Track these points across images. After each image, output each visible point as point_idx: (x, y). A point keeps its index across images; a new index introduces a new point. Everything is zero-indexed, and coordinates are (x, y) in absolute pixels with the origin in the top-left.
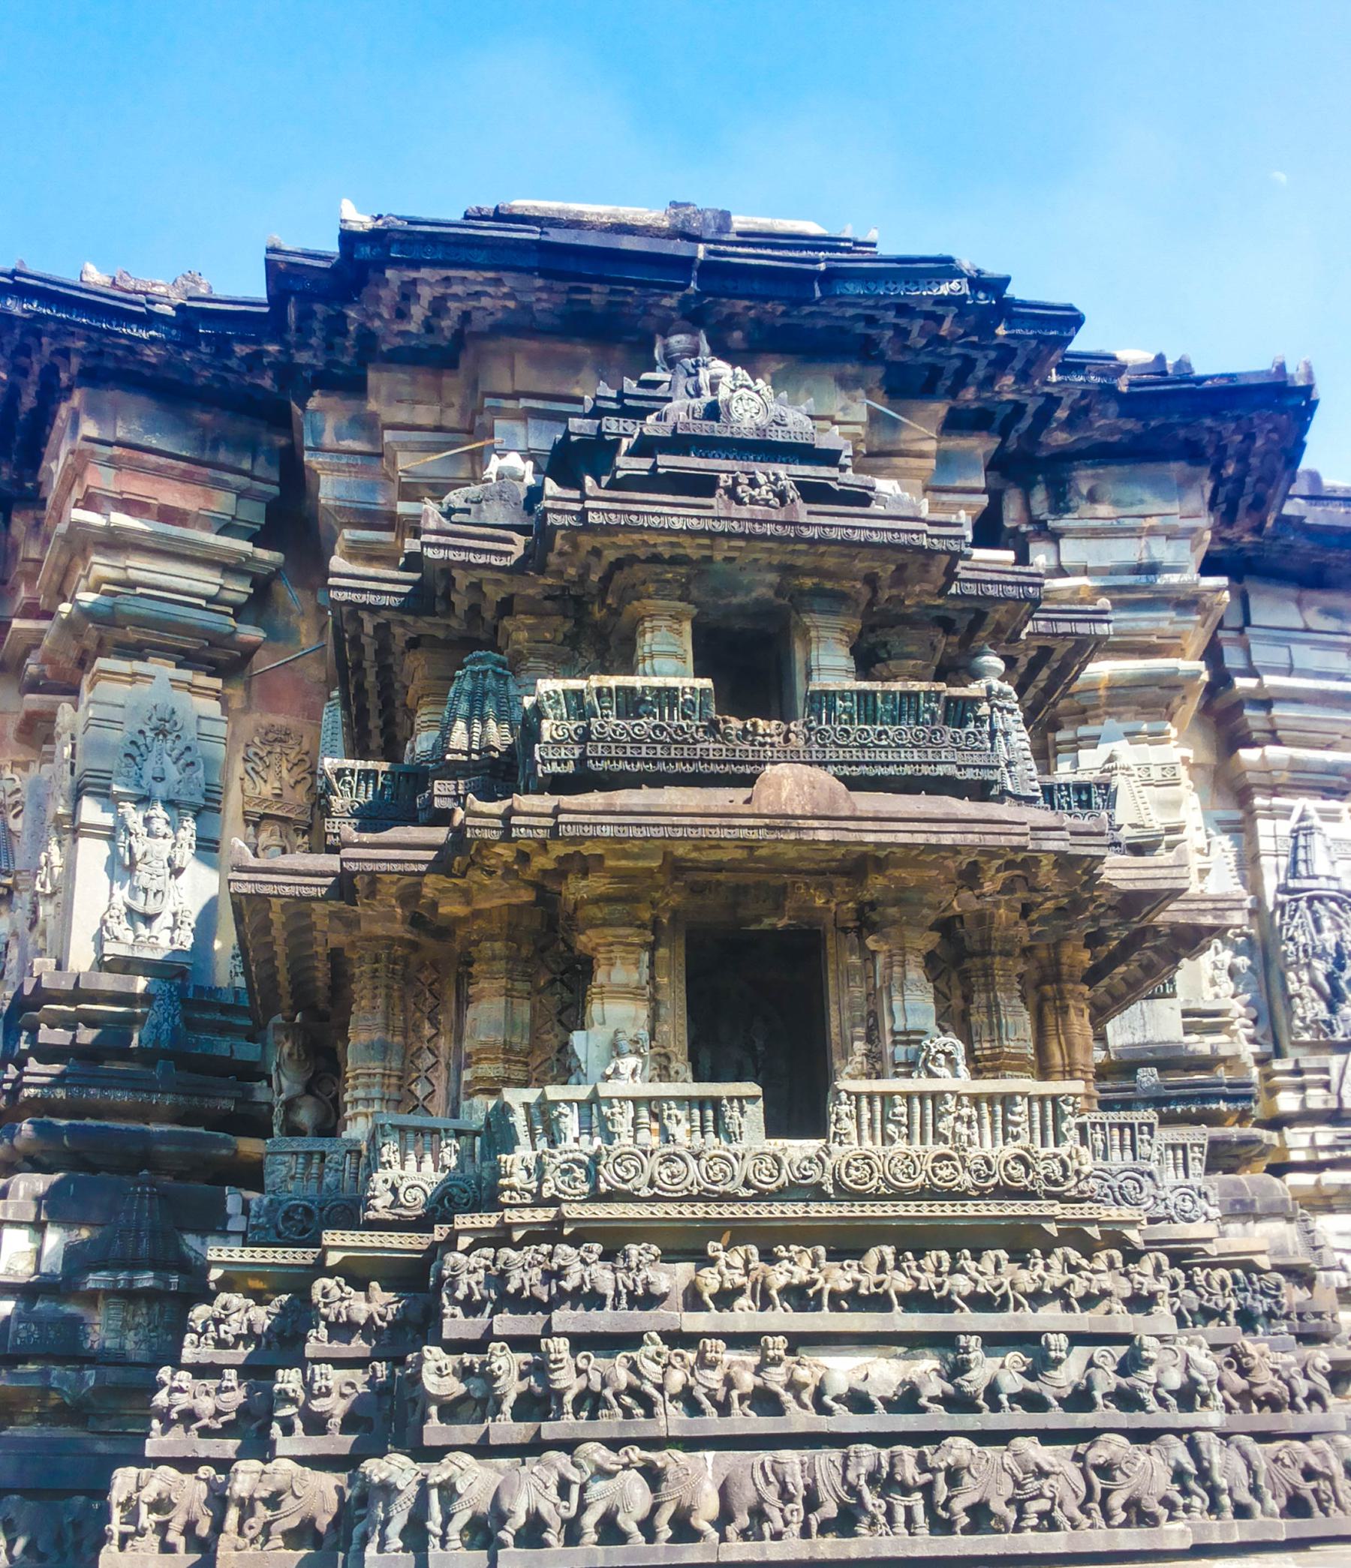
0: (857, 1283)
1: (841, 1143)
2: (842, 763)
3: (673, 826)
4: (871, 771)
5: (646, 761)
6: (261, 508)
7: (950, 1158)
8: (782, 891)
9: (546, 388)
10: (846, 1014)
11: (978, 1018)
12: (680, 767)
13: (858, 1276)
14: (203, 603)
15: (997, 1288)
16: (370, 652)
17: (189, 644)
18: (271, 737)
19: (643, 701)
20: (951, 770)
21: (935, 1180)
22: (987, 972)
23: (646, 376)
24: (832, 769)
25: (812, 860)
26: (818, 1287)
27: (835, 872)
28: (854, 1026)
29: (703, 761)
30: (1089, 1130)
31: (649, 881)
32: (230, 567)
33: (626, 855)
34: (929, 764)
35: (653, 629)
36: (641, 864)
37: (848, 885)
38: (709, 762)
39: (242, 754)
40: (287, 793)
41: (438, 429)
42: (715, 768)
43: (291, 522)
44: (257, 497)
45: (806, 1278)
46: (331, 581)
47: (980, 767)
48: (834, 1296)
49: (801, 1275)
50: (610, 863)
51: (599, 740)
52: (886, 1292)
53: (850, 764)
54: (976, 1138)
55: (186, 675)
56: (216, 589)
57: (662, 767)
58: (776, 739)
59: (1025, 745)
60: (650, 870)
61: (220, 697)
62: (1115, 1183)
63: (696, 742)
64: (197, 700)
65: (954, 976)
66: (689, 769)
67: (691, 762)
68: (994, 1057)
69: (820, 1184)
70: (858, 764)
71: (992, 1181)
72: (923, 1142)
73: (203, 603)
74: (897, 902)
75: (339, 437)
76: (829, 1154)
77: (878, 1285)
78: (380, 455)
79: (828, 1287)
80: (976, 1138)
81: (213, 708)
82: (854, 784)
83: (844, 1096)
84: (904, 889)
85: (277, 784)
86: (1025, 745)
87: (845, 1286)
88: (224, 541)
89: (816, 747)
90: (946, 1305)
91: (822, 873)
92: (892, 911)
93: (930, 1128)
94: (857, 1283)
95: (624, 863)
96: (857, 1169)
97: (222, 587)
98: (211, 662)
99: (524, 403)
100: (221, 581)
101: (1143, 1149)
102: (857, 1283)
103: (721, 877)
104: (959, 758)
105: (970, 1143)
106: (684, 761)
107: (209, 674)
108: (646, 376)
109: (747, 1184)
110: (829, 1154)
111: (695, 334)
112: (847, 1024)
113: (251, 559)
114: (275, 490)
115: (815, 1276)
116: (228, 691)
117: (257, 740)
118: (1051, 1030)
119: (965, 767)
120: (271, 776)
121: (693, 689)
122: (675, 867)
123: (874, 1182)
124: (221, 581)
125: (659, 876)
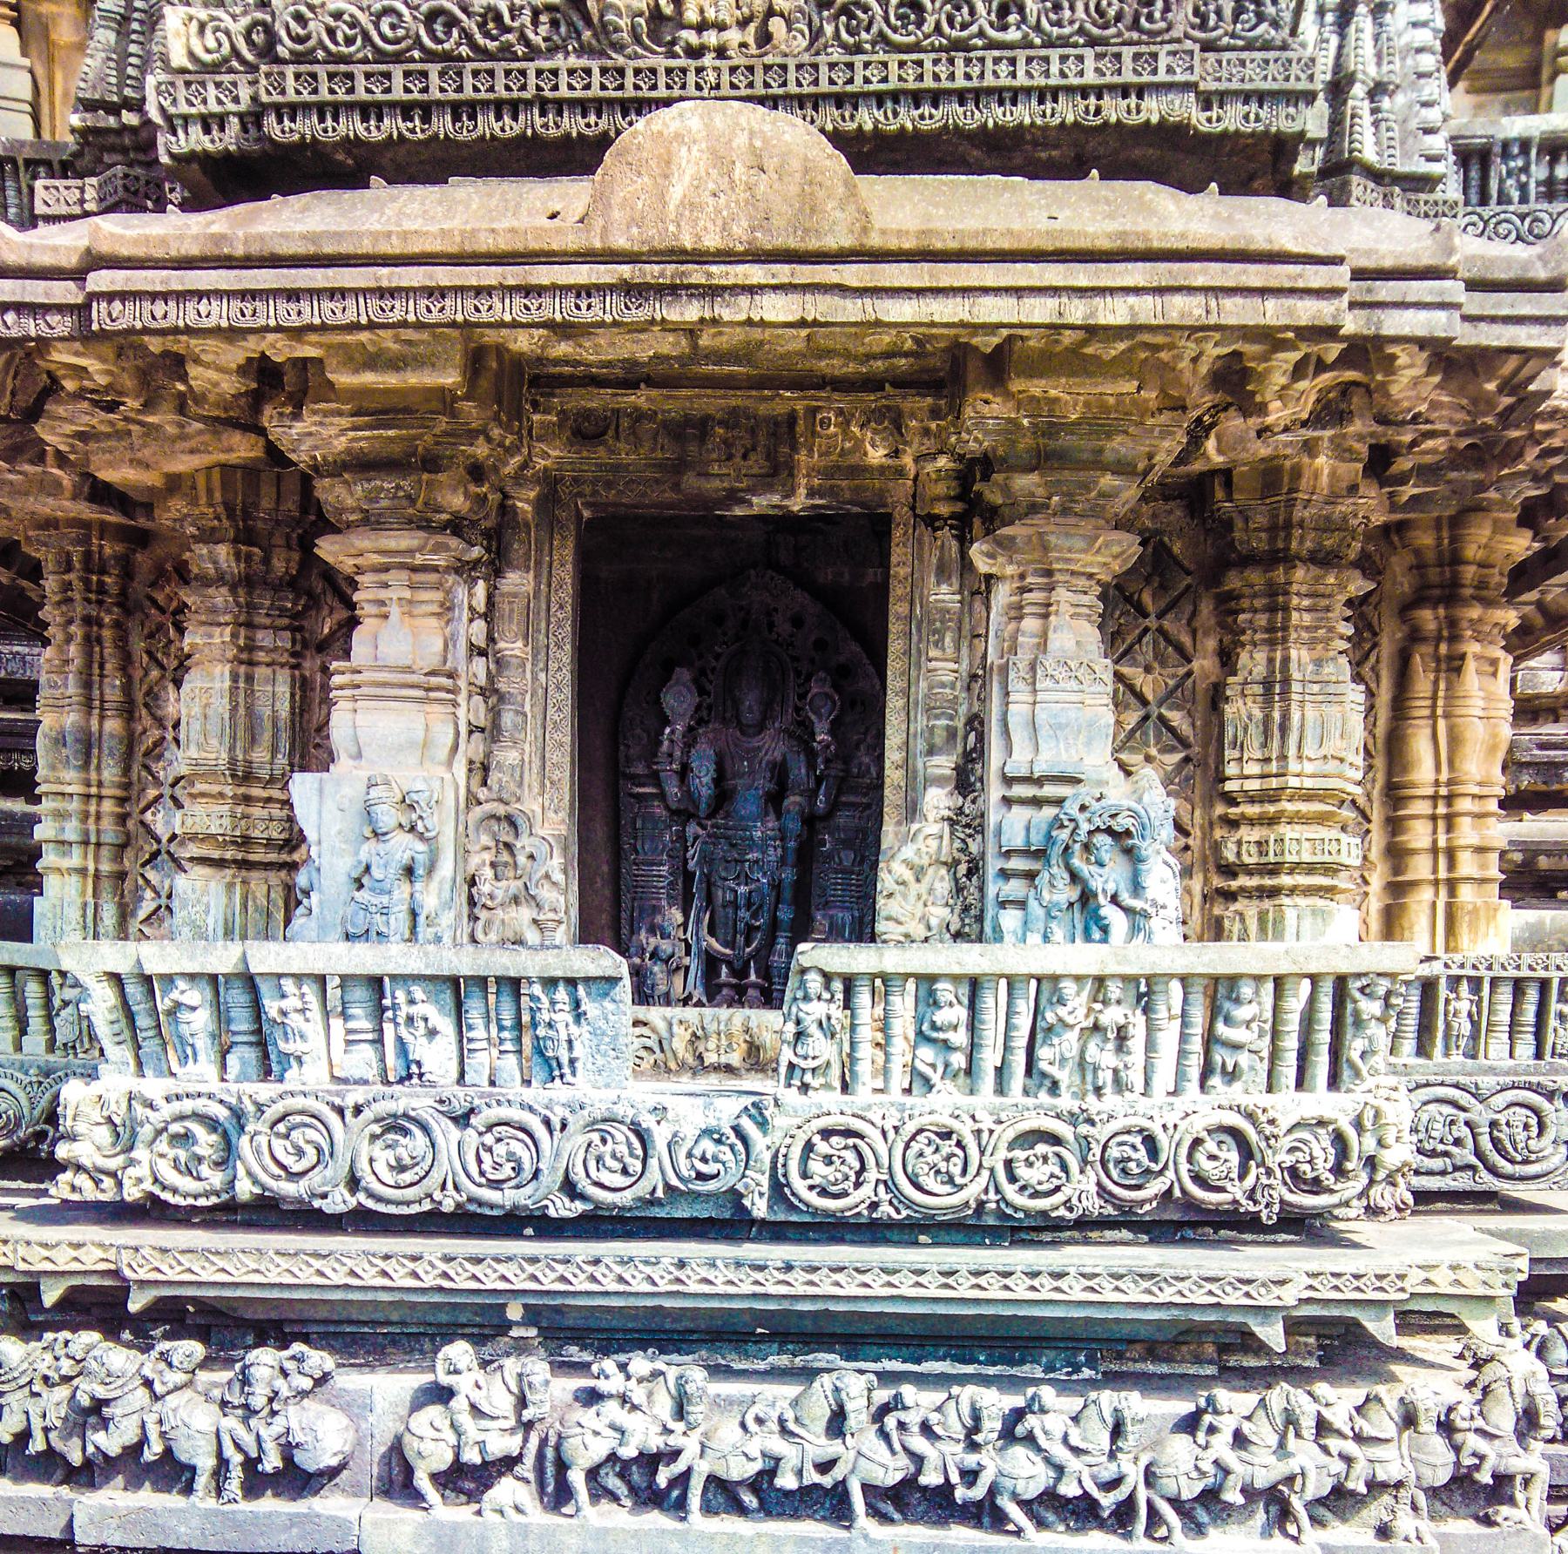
0: (773, 1466)
1: (805, 1088)
2: (895, 96)
3: (381, 292)
4: (968, 118)
8: (785, 430)
20: (1185, 109)
24: (830, 116)
25: (848, 355)
26: (679, 1467)
27: (903, 383)
29: (544, 105)
31: (443, 424)
33: (373, 361)
34: (1124, 91)
36: (413, 379)
37: (935, 413)
38: (560, 105)
45: (655, 1443)
47: (1261, 97)
48: (715, 1482)
49: (643, 1434)
50: (344, 379)
51: (298, 58)
53: (917, 98)
54: (1136, 1077)
58: (733, 36)
59: (1424, 36)
60: (441, 391)
63: (533, 53)
66: (510, 128)
67: (515, 107)
69: (735, 1196)
70: (936, 97)
72: (1000, 1090)
74: (1041, 460)
76: (763, 1124)
79: (702, 1469)
80: (1136, 1077)
82: (872, 154)
83: (814, 982)
84: (1052, 430)
86: (1424, 36)
87: (740, 1470)
89: (837, 55)
91: (871, 384)
92: (1026, 482)
94: (773, 1466)
95: (369, 378)
96: (828, 1160)
103: (640, 399)
104: (1207, 73)
105: (1120, 1085)
106: (499, 107)
110: (763, 1124)
115: (674, 1441)
119: (1223, 97)
122: (511, 383)
123: (866, 1191)
125: (467, 406)
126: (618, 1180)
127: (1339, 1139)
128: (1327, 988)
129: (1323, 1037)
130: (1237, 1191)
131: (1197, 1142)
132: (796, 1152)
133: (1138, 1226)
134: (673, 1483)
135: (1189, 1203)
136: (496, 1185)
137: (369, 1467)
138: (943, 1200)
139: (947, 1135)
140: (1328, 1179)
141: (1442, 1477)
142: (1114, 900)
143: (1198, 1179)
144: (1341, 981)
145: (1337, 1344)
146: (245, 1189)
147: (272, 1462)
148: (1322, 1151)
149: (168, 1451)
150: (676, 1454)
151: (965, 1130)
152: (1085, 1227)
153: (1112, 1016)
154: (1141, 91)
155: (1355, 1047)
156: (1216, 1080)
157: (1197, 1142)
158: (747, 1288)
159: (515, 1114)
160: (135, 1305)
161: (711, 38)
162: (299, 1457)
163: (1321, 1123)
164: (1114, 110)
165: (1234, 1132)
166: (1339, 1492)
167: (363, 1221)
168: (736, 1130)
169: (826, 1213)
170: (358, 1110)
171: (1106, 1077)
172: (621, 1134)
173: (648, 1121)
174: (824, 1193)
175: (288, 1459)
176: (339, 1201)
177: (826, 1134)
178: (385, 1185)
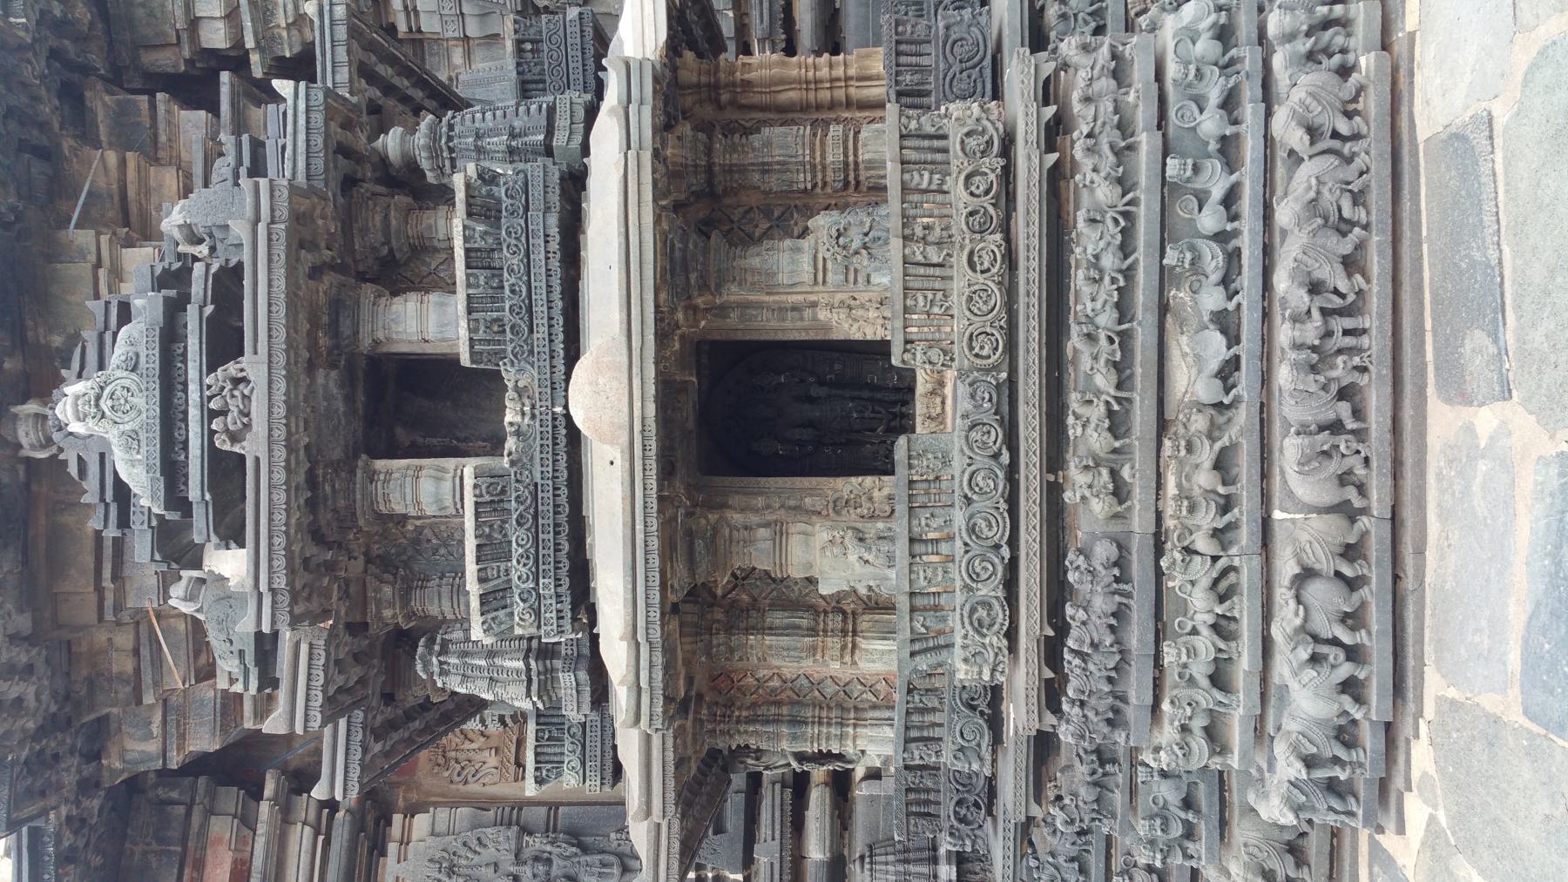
5: (557, 533)
6: (222, 790)
7: (971, 254)
9: (89, 561)
10: (788, 324)
11: (774, 182)
12: (563, 499)
13: (1102, 361)
14: (321, 838)
15: (1116, 221)
16: (396, 736)
17: (364, 849)
18: (441, 761)
19: (489, 536)
21: (994, 270)
22: (729, 170)
23: (73, 470)
28: (802, 319)
30: (902, 87)
32: (285, 816)
35: (387, 501)
39: (460, 786)
40: (494, 742)
41: (136, 652)
42: (562, 464)
43: (240, 765)
44: (212, 796)
46: (299, 730)
52: (1119, 333)
55: (392, 848)
56: (307, 829)
57: (563, 518)
61: (412, 811)
62: (956, 68)
64: (415, 835)
65: (728, 201)
68: (814, 167)
71: (991, 210)
73: (321, 838)
75: (149, 736)
77: (1111, 341)
78: (165, 701)
81: (421, 822)
83: (907, 356)
85: (486, 753)
88: (262, 829)
90: (1129, 273)
93: (938, 271)
96: (982, 348)
97: (304, 823)
98: (377, 824)
99: (107, 583)
100: (299, 825)
101: (921, 30)
102: (1108, 361)
107: (389, 823)
108: (73, 470)
109: (996, 456)
111: (16, 416)
112: (799, 324)
113: (275, 799)
114: (202, 781)
116: (401, 803)
117: (446, 774)
118: (766, 99)
120: (478, 757)
121: (475, 486)
124: (299, 825)
126: (993, 433)
127: (968, 134)
128: (906, 143)
129: (926, 143)
130: (992, 177)
131: (972, 194)
132: (979, 361)
133: (1008, 217)
134: (1119, 403)
135: (997, 197)
136: (996, 488)
137: (1115, 528)
138: (998, 297)
139: (970, 299)
140: (986, 137)
141: (1113, 83)
142: (866, 234)
143: (987, 192)
144: (902, 137)
145: (1056, 131)
146: (1000, 593)
147: (1116, 572)
148: (972, 142)
149: (1114, 615)
150: (1107, 403)
151: (967, 292)
152: (1008, 239)
153: (919, 232)
154: (546, 236)
155: (931, 130)
156: (945, 188)
157: (972, 194)
158: (1036, 377)
159: (966, 477)
160: (1052, 633)
161: (527, 409)
162: (1113, 559)
163: (962, 142)
164: (554, 245)
165: (968, 177)
166: (1119, 126)
167: (1013, 542)
168: (971, 385)
169: (1005, 347)
170: (966, 544)
171: (945, 234)
172: (973, 434)
173: (968, 422)
174: (996, 349)
175: (1116, 564)
176: (1006, 552)
177: (971, 348)
178: (1000, 533)
